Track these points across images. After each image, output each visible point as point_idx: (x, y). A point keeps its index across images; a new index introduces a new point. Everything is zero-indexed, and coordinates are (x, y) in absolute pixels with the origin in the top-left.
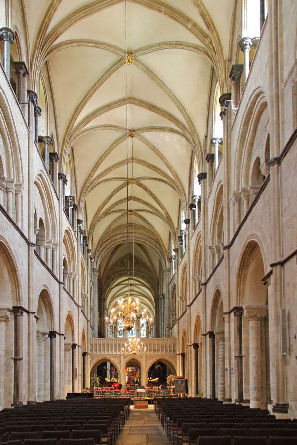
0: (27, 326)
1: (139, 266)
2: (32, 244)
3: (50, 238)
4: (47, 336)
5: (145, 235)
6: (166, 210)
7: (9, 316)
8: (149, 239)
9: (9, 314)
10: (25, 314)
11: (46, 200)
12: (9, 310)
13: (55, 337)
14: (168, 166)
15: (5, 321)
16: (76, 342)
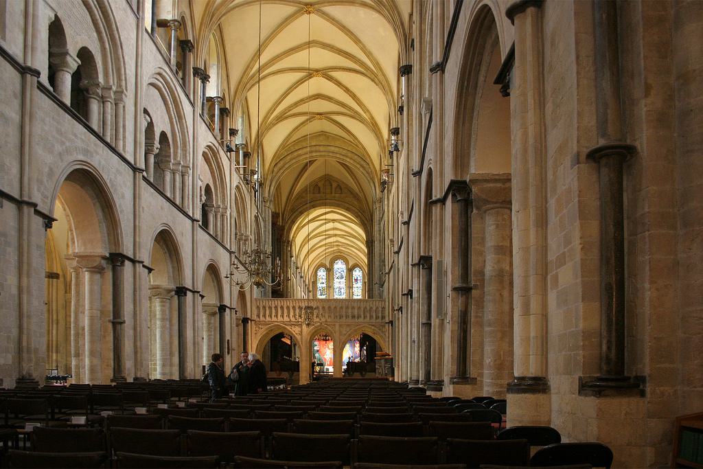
0: (131, 280)
1: (341, 193)
2: (139, 169)
3: (179, 159)
4: (174, 293)
7: (105, 266)
8: (349, 154)
10: (127, 262)
13: (186, 295)
15: (100, 273)
16: (227, 302)
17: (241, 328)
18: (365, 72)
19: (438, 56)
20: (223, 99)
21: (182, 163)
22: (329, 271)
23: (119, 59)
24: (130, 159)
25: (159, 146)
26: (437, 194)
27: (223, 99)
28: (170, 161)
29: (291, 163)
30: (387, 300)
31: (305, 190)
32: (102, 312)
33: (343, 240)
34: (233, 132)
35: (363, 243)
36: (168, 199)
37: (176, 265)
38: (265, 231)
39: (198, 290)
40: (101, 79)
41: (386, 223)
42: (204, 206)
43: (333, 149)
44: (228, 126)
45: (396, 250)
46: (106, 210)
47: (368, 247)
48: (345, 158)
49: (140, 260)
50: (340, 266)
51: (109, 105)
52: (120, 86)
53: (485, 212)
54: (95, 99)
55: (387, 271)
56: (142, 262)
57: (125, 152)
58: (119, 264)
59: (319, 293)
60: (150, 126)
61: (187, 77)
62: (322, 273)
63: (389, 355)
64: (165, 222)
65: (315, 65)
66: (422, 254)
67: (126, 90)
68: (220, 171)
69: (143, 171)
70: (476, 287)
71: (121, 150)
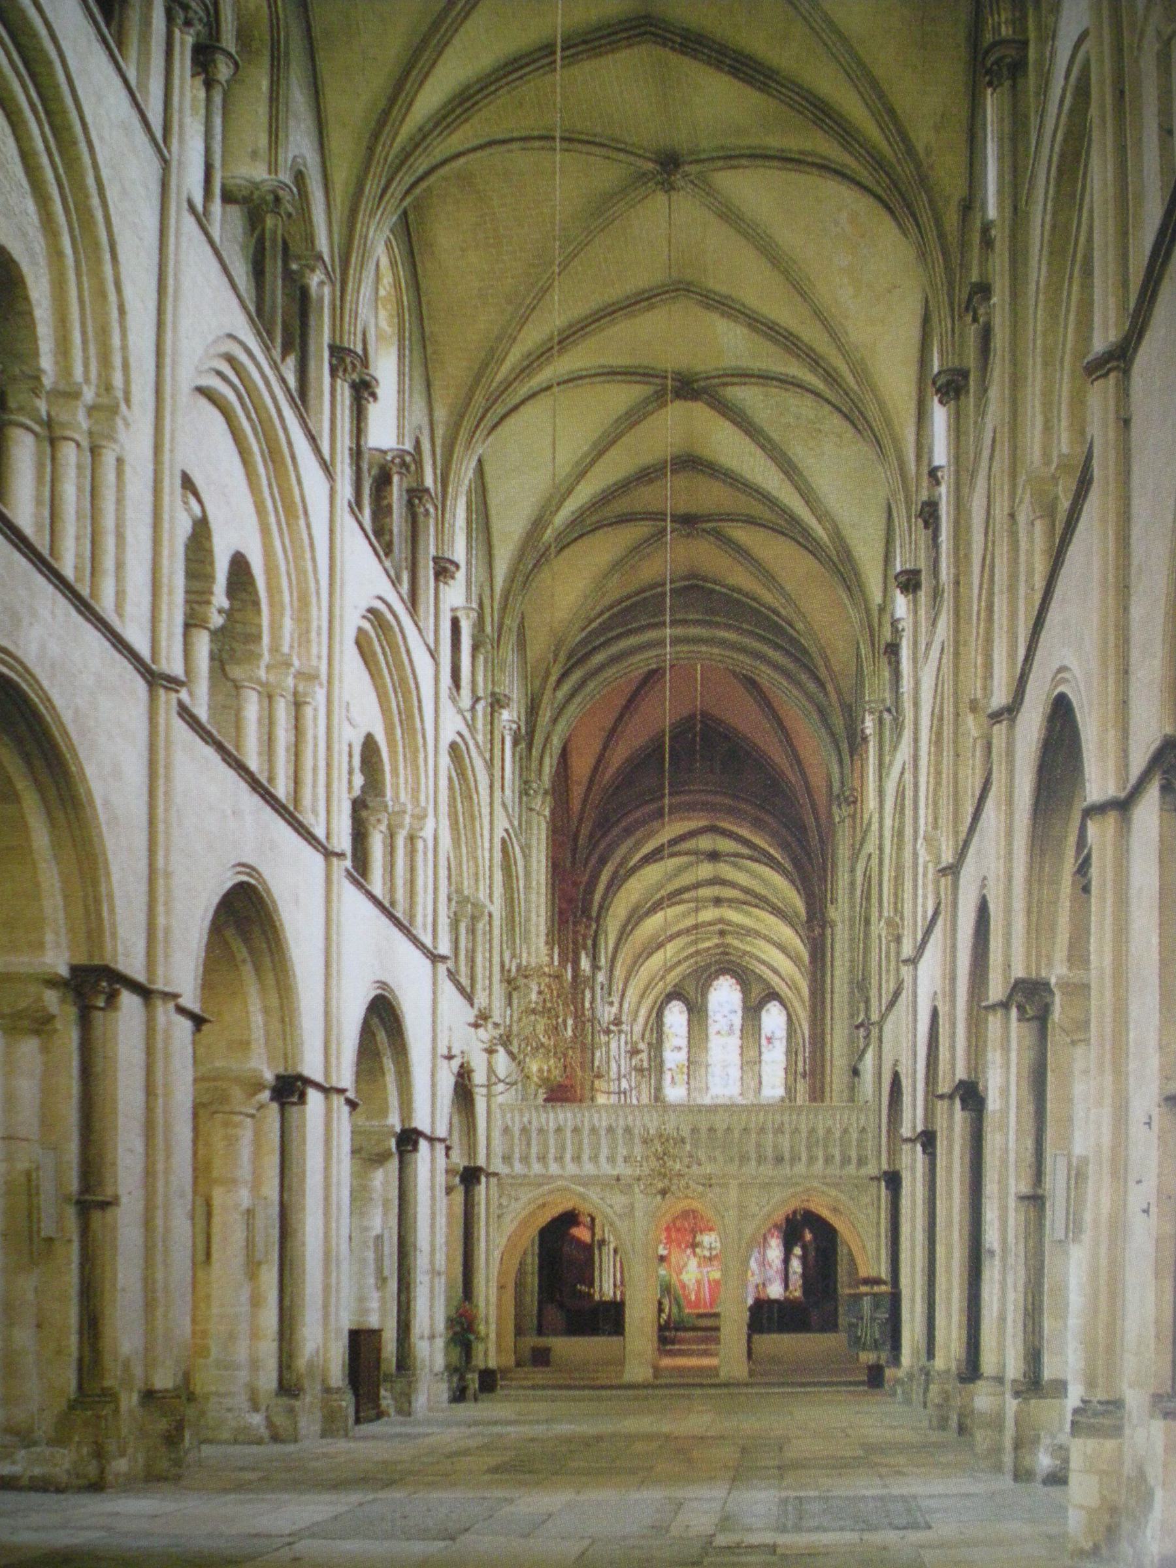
9: (51, 998)
12: (53, 982)
16: (421, 1121)
17: (459, 1196)
21: (296, 663)
24: (140, 642)
25: (225, 604)
36: (255, 784)
37: (274, 1001)
39: (342, 1085)
40: (46, 362)
41: (875, 861)
42: (358, 806)
46: (60, 816)
49: (167, 989)
51: (69, 453)
52: (108, 388)
54: (28, 428)
56: (175, 996)
57: (120, 615)
58: (102, 1004)
60: (201, 531)
64: (244, 860)
67: (127, 401)
69: (180, 683)
71: (106, 605)
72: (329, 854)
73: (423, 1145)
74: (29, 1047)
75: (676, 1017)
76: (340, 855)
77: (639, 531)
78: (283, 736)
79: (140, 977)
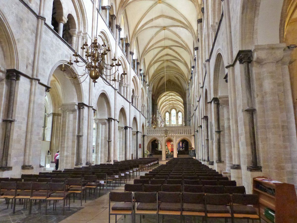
0: (114, 126)
1: (174, 86)
3: (125, 83)
4: (124, 129)
5: (175, 71)
6: (184, 60)
7: (106, 122)
8: (177, 73)
9: (106, 121)
10: (113, 121)
11: (123, 65)
12: (106, 120)
13: (127, 129)
14: (183, 41)
15: (105, 124)
16: (139, 130)
18: (182, 47)
19: (208, 57)
20: (138, 60)
22: (170, 113)
23: (111, 55)
26: (209, 100)
27: (138, 60)
28: (123, 84)
29: (158, 77)
30: (192, 127)
31: (163, 84)
32: (105, 138)
33: (175, 102)
34: (140, 70)
35: (182, 104)
38: (149, 102)
42: (132, 96)
43: (172, 72)
44: (139, 68)
45: (195, 109)
47: (184, 105)
48: (176, 75)
50: (174, 112)
53: (224, 107)
55: (192, 116)
59: (166, 122)
61: (128, 55)
62: (167, 114)
63: (193, 148)
65: (166, 45)
66: (205, 115)
68: (137, 84)
70: (222, 131)
72: (130, 103)
73: (139, 133)
74: (104, 126)
75: (167, 114)
76: (131, 103)
77: (161, 62)
78: (125, 91)
79: (114, 118)
